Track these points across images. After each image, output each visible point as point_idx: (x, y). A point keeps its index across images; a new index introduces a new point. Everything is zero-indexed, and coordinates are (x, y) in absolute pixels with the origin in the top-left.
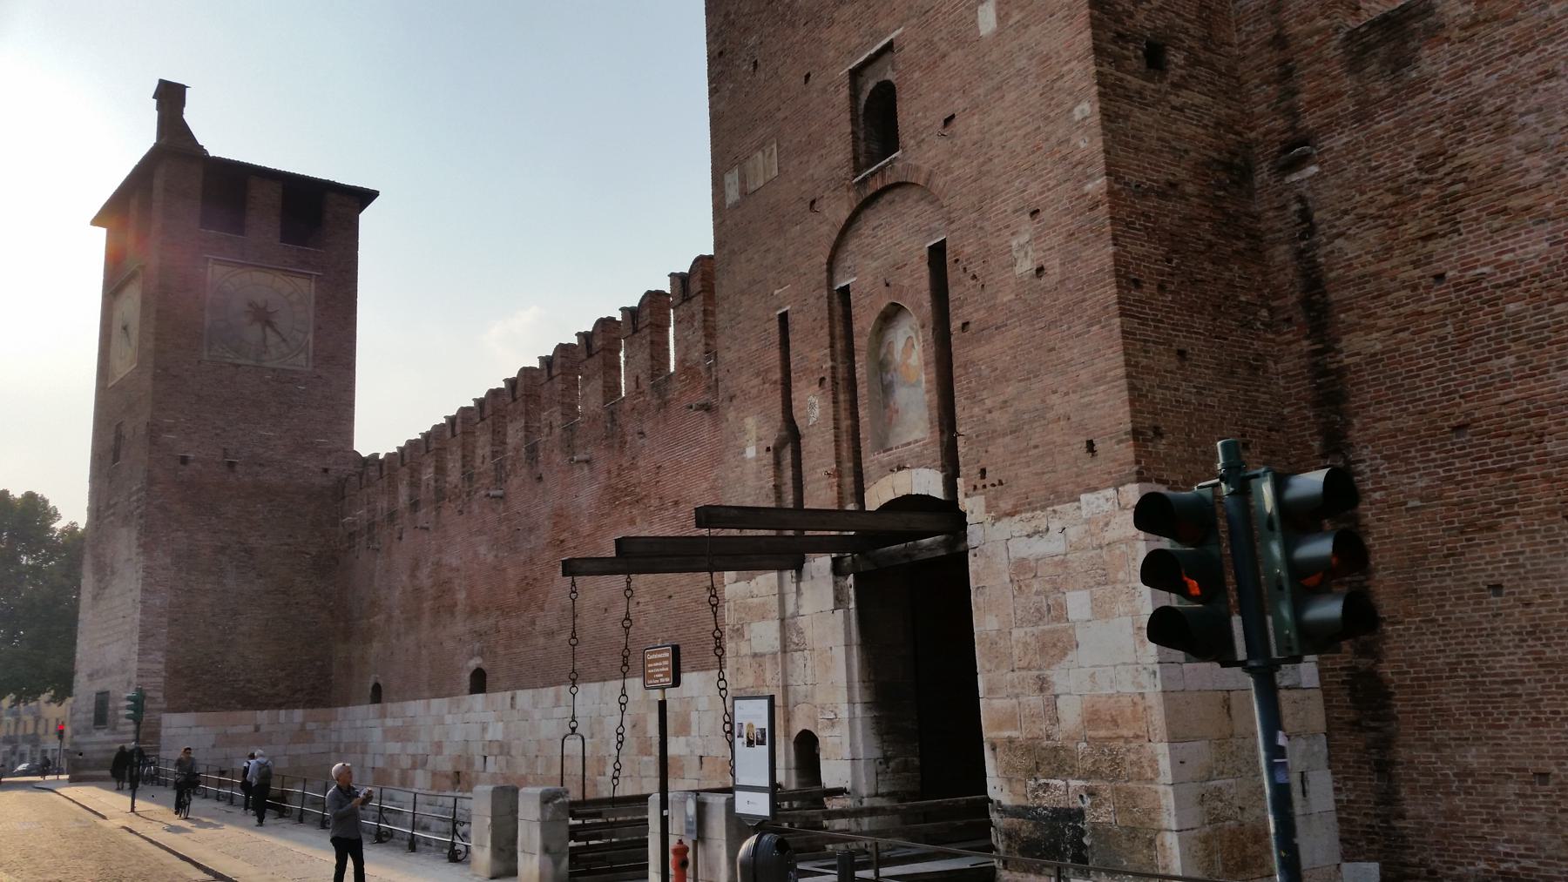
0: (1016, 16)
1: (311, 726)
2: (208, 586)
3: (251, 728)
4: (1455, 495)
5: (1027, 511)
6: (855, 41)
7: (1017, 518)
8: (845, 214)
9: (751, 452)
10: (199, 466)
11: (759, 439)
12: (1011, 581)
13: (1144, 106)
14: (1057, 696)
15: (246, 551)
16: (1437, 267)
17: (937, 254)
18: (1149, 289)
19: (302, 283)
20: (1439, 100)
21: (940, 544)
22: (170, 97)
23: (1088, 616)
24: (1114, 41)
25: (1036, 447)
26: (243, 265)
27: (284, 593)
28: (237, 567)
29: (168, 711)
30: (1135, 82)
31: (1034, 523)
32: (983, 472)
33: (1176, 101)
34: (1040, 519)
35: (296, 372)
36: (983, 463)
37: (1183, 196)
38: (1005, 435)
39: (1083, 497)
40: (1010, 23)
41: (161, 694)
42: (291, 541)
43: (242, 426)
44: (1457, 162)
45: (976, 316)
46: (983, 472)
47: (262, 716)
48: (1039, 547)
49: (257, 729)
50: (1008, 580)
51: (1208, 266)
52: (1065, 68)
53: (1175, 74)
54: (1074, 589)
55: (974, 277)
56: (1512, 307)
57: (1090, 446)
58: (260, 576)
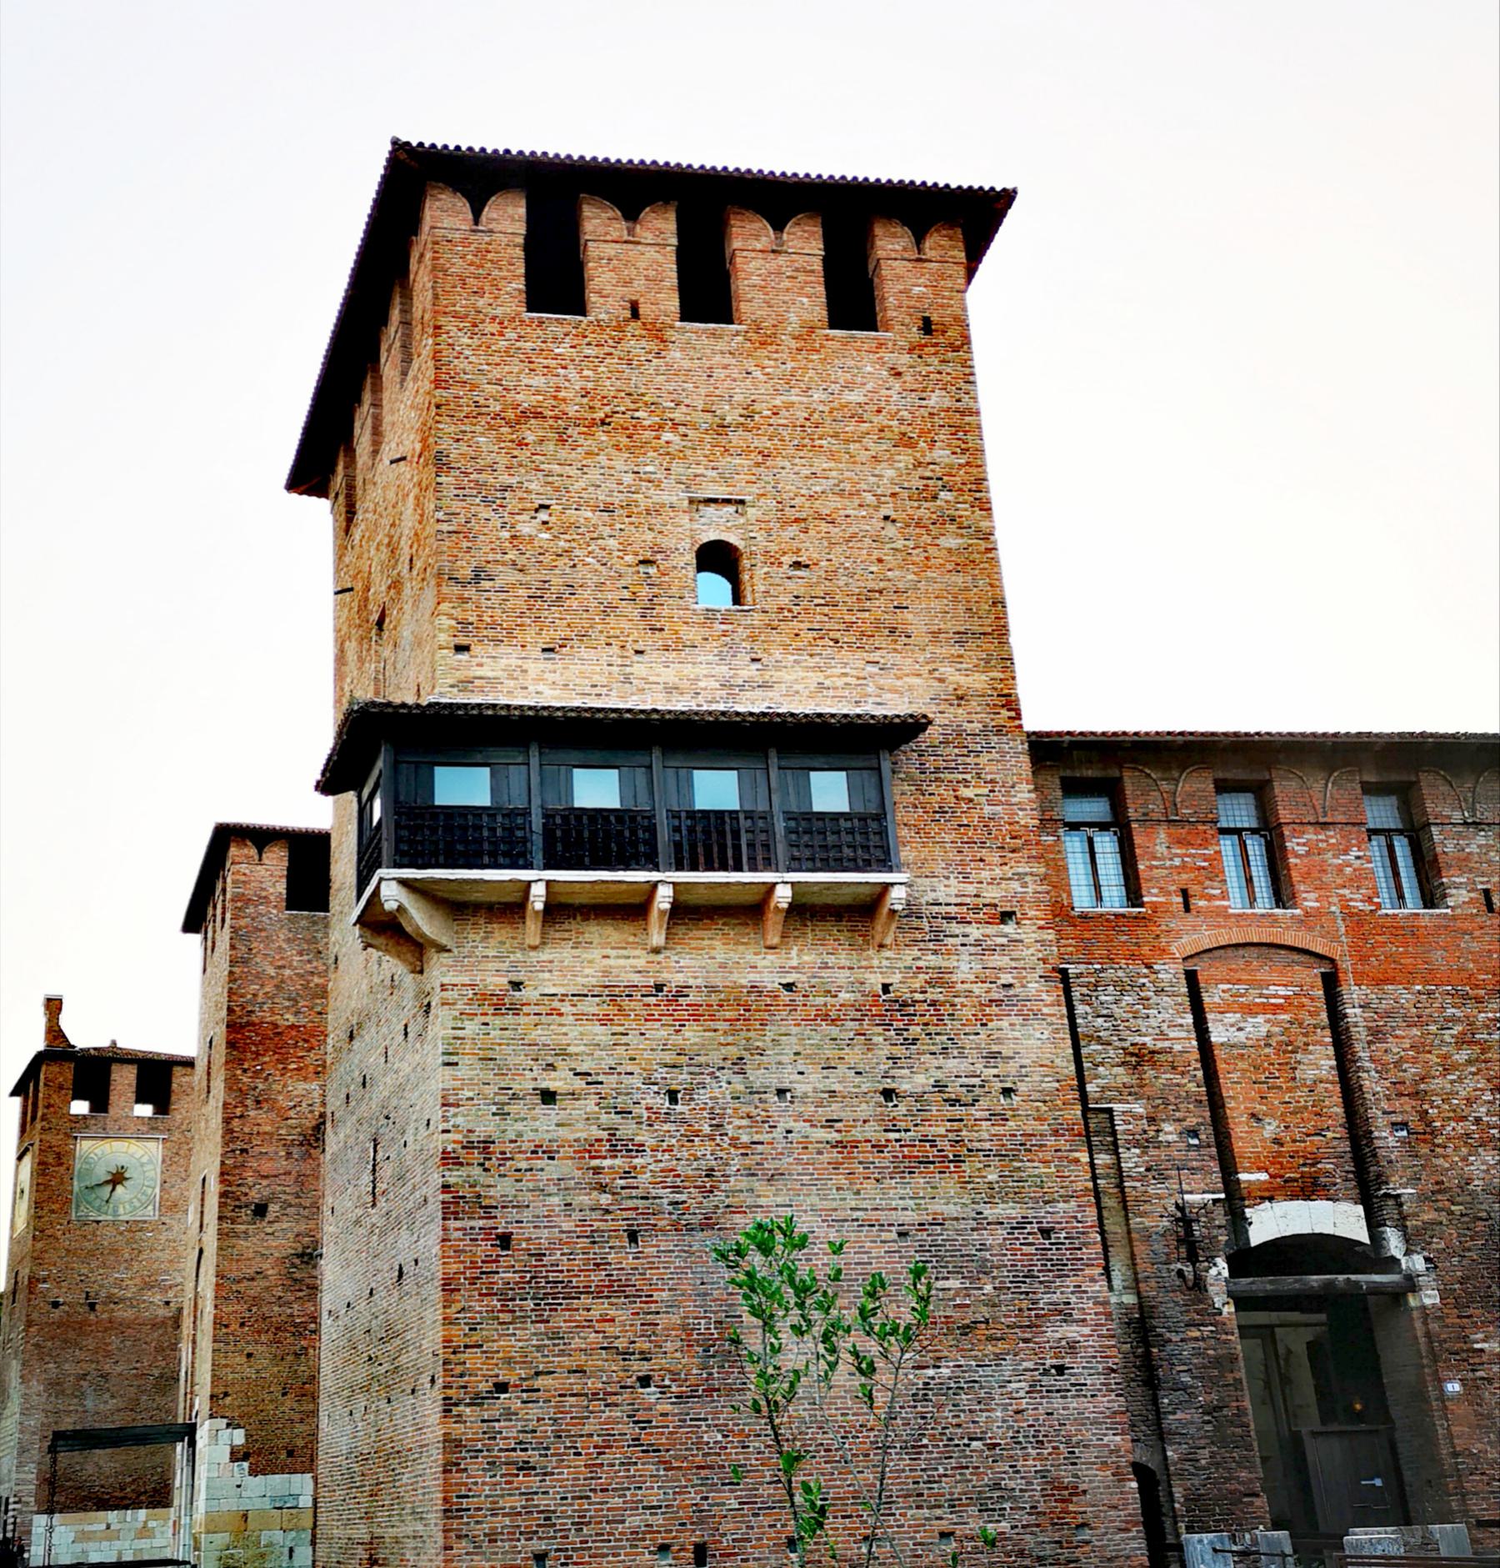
1: (152, 1524)
2: (71, 1408)
3: (104, 1526)
10: (66, 1308)
13: (246, 1239)
15: (101, 1376)
18: (234, 1326)
19: (152, 1145)
22: (54, 1006)
24: (233, 1211)
26: (103, 1138)
27: (132, 1410)
28: (95, 1390)
29: (38, 1513)
30: (243, 1227)
33: (269, 1230)
35: (145, 1222)
37: (266, 1277)
41: (32, 1499)
42: (138, 1365)
43: (101, 1271)
47: (112, 1516)
49: (108, 1527)
51: (276, 1309)
53: (270, 1216)
58: (113, 1397)
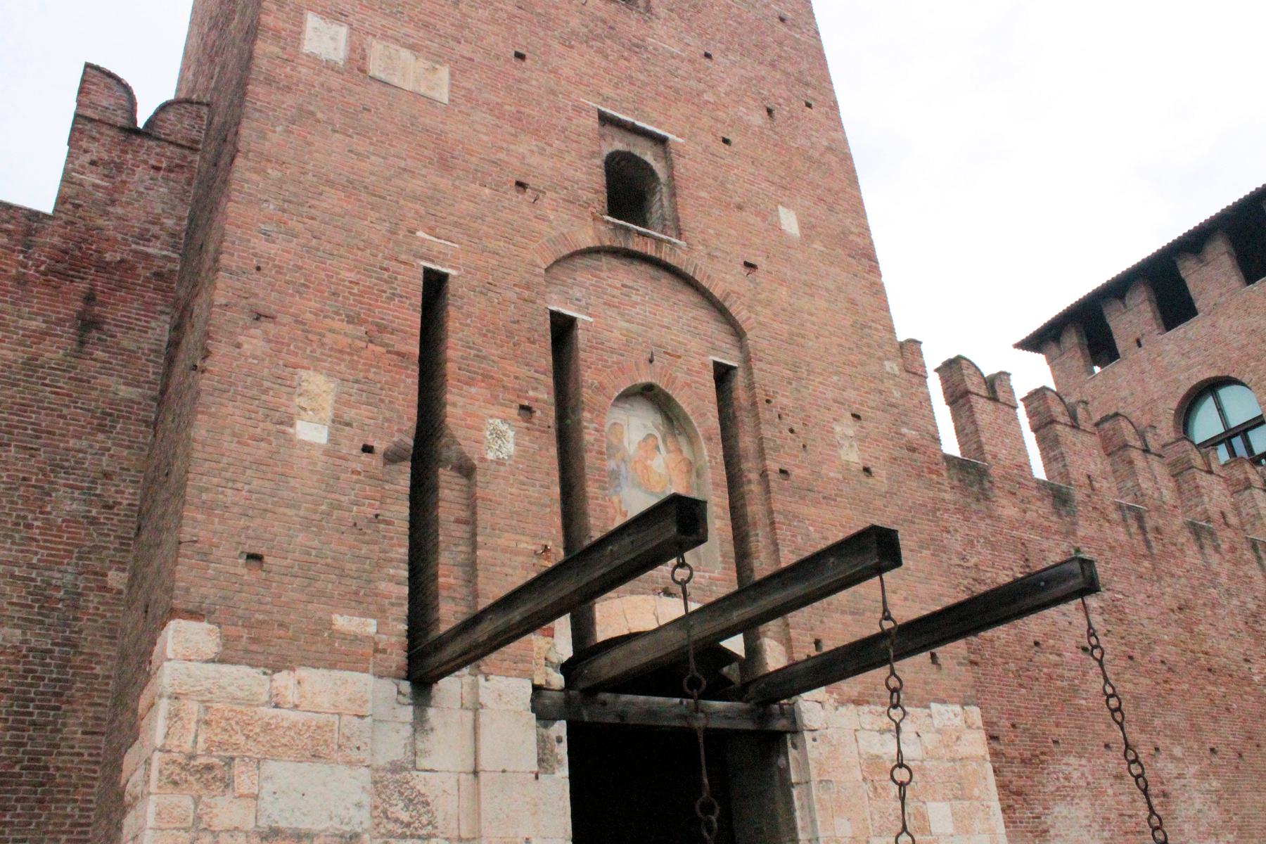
0: (818, 246)
5: (875, 704)
6: (608, 91)
7: (865, 708)
11: (339, 422)
12: (864, 779)
17: (723, 375)
21: (741, 714)
23: (950, 830)
38: (843, 612)
39: (933, 705)
50: (860, 778)
52: (873, 324)
54: (934, 800)
55: (792, 431)
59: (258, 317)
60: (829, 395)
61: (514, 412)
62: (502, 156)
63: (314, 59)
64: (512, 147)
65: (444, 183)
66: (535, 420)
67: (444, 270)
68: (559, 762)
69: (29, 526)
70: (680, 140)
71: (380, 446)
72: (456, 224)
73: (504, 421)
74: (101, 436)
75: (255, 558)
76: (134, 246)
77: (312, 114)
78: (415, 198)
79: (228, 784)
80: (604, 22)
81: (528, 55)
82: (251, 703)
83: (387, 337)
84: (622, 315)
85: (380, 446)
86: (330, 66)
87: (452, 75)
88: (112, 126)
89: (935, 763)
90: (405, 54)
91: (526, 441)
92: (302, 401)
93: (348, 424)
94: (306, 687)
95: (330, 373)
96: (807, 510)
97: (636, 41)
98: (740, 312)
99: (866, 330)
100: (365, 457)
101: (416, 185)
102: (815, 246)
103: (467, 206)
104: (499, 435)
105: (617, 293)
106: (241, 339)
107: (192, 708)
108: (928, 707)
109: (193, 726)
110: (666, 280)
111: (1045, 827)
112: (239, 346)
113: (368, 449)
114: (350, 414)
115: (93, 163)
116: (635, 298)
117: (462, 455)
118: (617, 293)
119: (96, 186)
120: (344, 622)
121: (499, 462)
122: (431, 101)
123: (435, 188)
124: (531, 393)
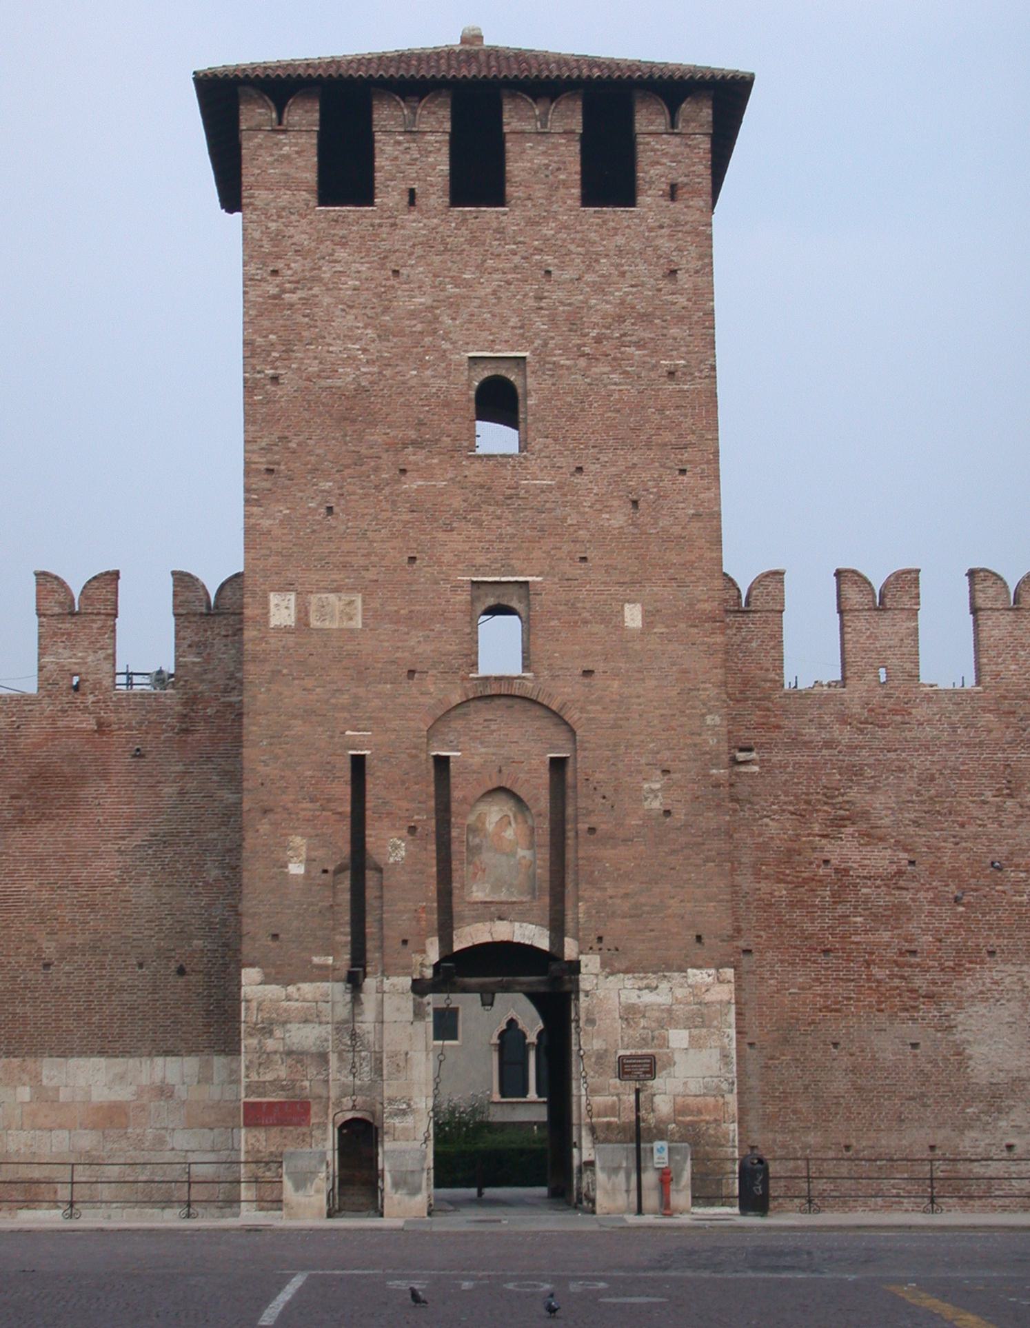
0: (660, 629)
4: (819, 989)
5: (639, 972)
6: (480, 560)
8: (456, 698)
9: (296, 869)
11: (309, 861)
14: (654, 1095)
16: (828, 856)
17: (558, 765)
20: (841, 758)
21: (540, 982)
25: (652, 930)
31: (645, 982)
32: (600, 939)
34: (652, 979)
36: (600, 933)
38: (624, 917)
39: (689, 970)
40: (655, 630)
44: (845, 798)
45: (603, 826)
46: (600, 939)
48: (648, 998)
52: (702, 686)
56: (864, 890)
57: (699, 938)
59: (266, 812)
60: (643, 761)
61: (404, 832)
62: (398, 655)
63: (278, 629)
64: (406, 644)
65: (361, 691)
66: (417, 834)
67: (363, 753)
68: (429, 1014)
69: (196, 886)
70: (539, 579)
71: (331, 868)
72: (370, 718)
73: (399, 838)
74: (223, 829)
75: (275, 936)
76: (222, 700)
77: (280, 671)
78: (343, 708)
79: (271, 1033)
80: (482, 487)
81: (417, 555)
82: (278, 1001)
83: (332, 805)
84: (482, 743)
85: (331, 868)
86: (287, 630)
87: (364, 601)
88: (195, 615)
89: (682, 1006)
90: (332, 597)
91: (411, 848)
92: (290, 853)
93: (314, 860)
94: (302, 991)
95: (303, 836)
96: (609, 853)
97: (509, 492)
98: (573, 716)
99: (695, 693)
100: (324, 876)
101: (344, 699)
102: (655, 630)
103: (377, 703)
104: (396, 847)
105: (480, 727)
106: (258, 827)
107: (254, 1004)
108: (686, 972)
109: (255, 1012)
110: (518, 705)
111: (953, 1023)
112: (257, 831)
113: (325, 871)
114: (314, 854)
115: (190, 646)
116: (493, 727)
117: (375, 863)
118: (480, 727)
119: (194, 663)
120: (316, 960)
121: (396, 863)
122: (352, 631)
123: (356, 697)
124: (416, 817)
